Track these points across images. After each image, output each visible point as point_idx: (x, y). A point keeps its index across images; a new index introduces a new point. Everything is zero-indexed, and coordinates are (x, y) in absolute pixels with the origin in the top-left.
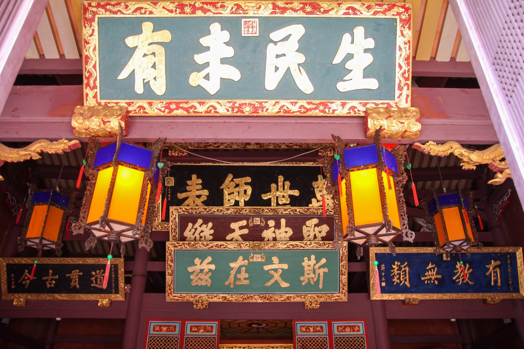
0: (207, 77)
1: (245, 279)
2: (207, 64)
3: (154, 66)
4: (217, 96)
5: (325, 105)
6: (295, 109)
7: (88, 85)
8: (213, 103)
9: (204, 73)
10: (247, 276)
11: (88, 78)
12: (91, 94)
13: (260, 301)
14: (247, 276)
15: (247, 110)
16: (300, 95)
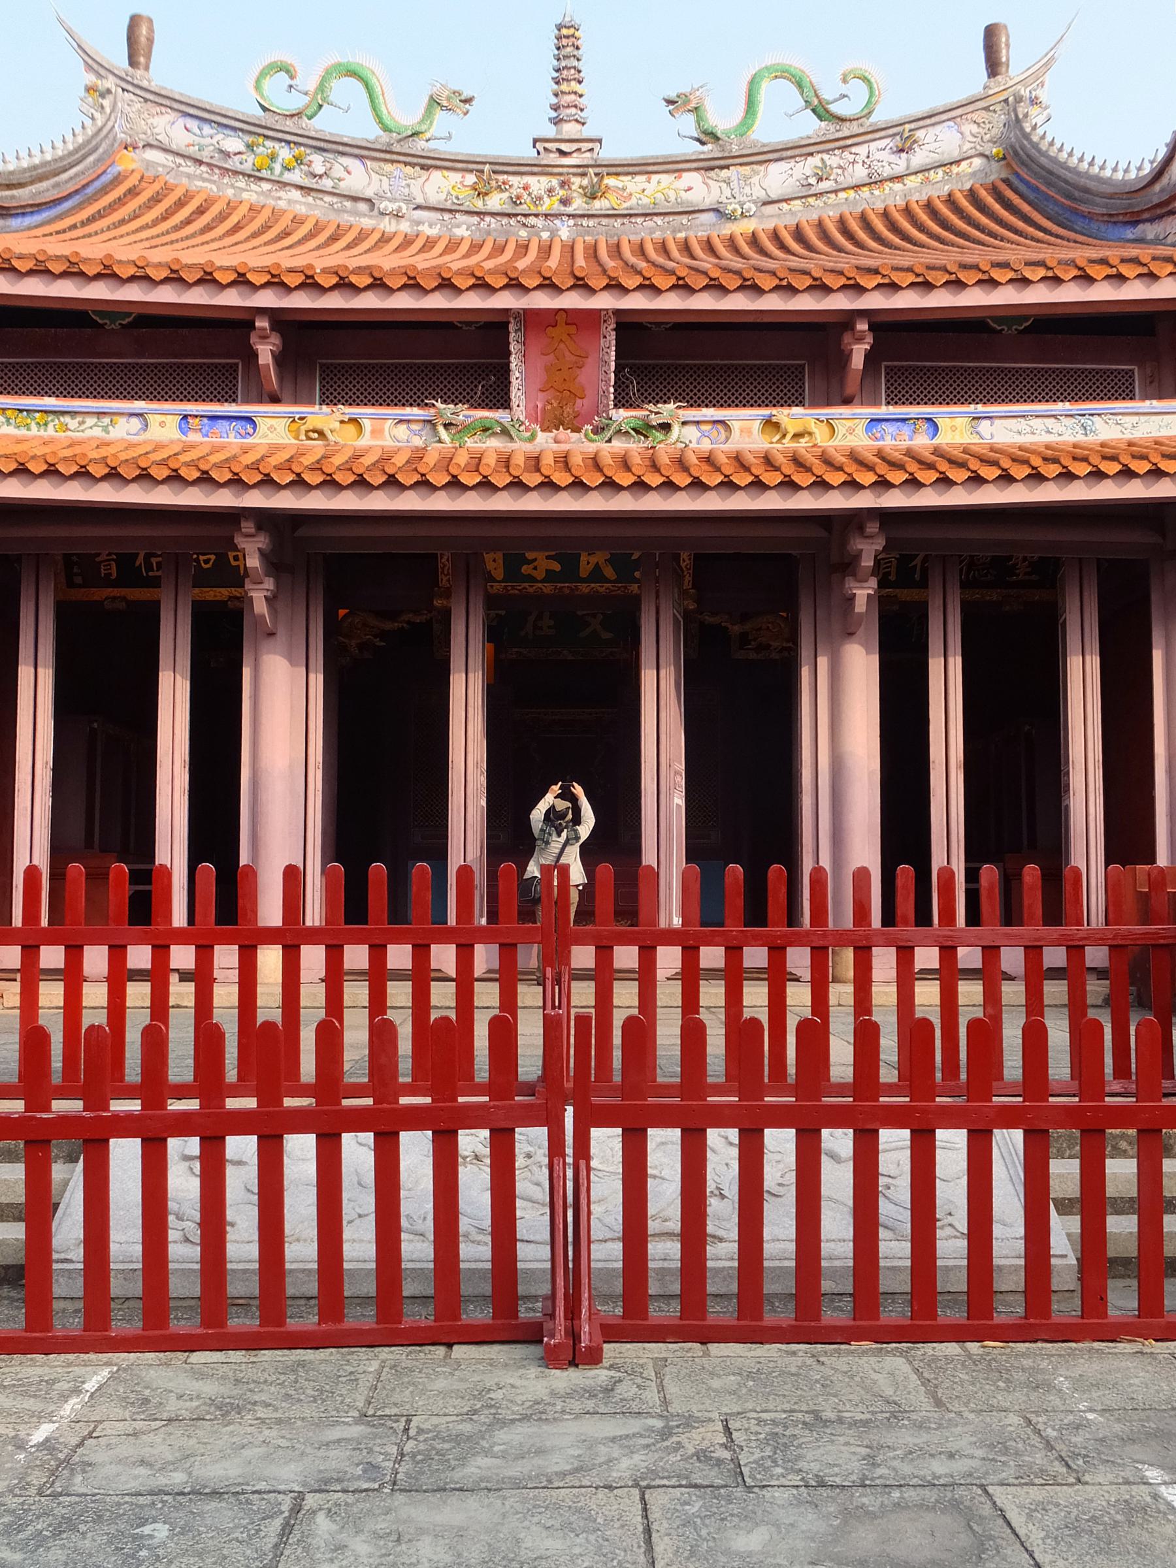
0: (535, 568)
1: (549, 627)
2: (536, 560)
3: (494, 561)
4: (542, 581)
5: (626, 588)
6: (602, 590)
7: (443, 572)
8: (540, 585)
9: (531, 566)
10: (552, 623)
11: (443, 569)
12: (445, 579)
13: (570, 657)
14: (552, 623)
15: (567, 591)
16: (604, 580)
